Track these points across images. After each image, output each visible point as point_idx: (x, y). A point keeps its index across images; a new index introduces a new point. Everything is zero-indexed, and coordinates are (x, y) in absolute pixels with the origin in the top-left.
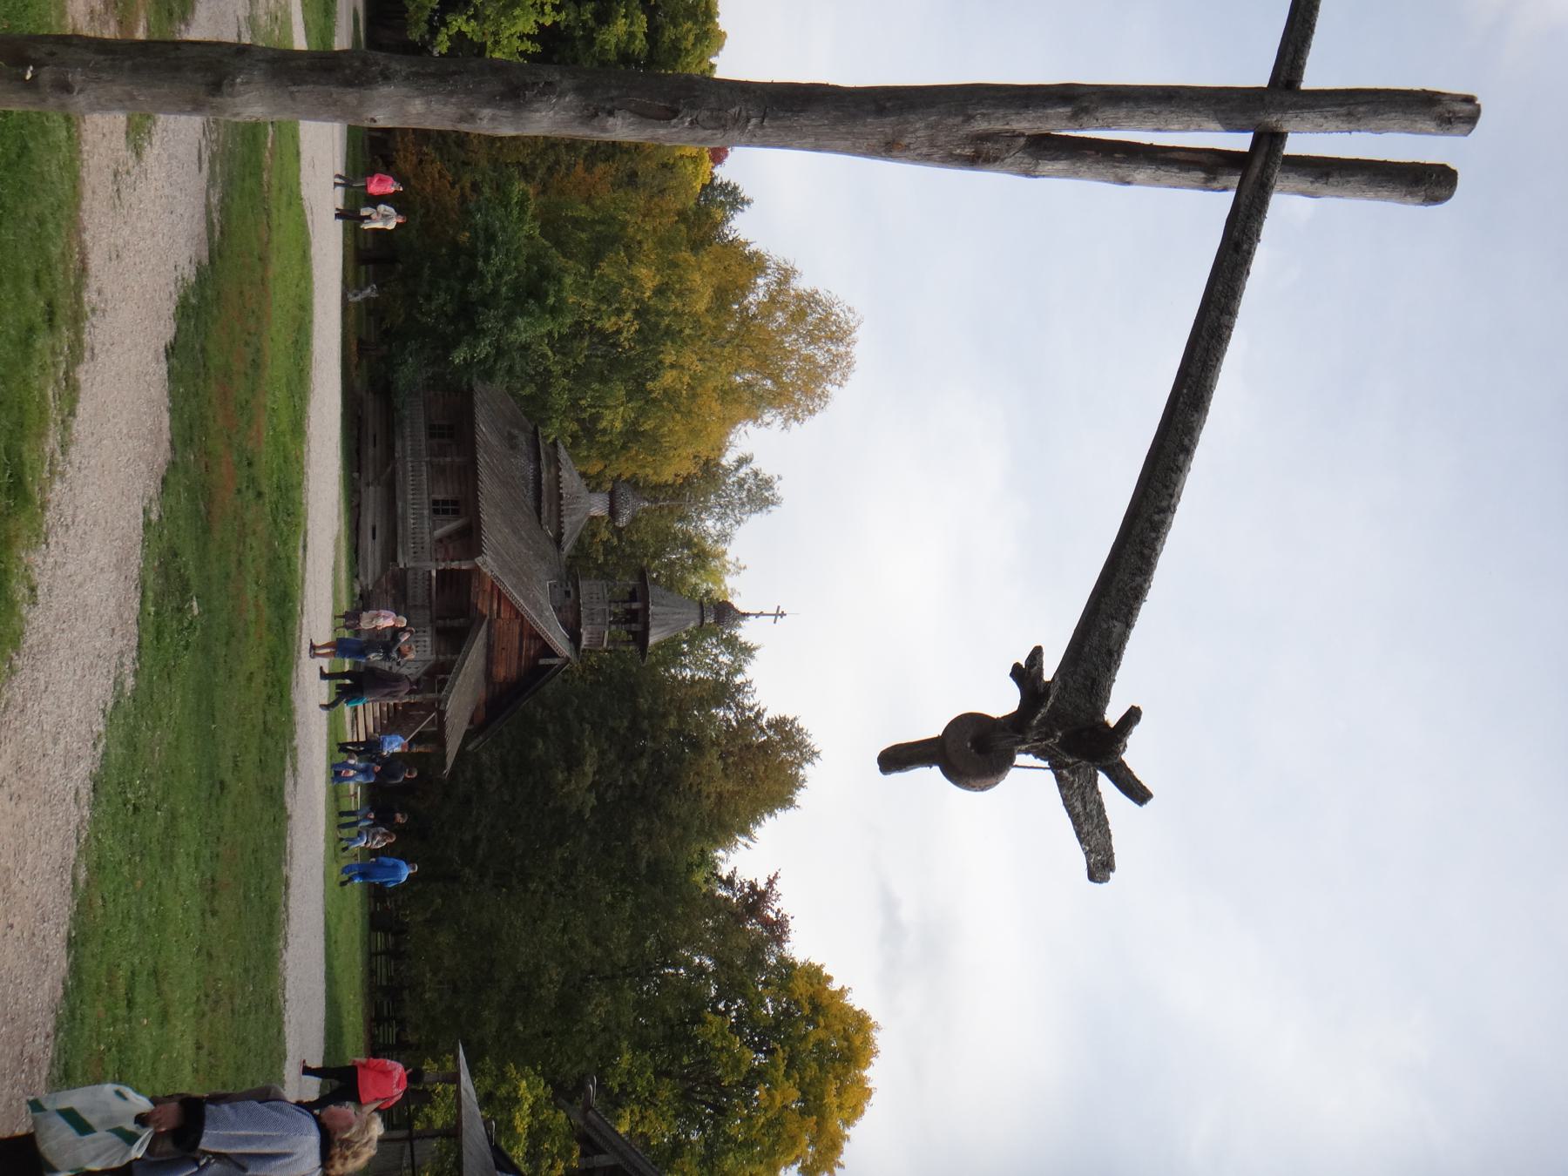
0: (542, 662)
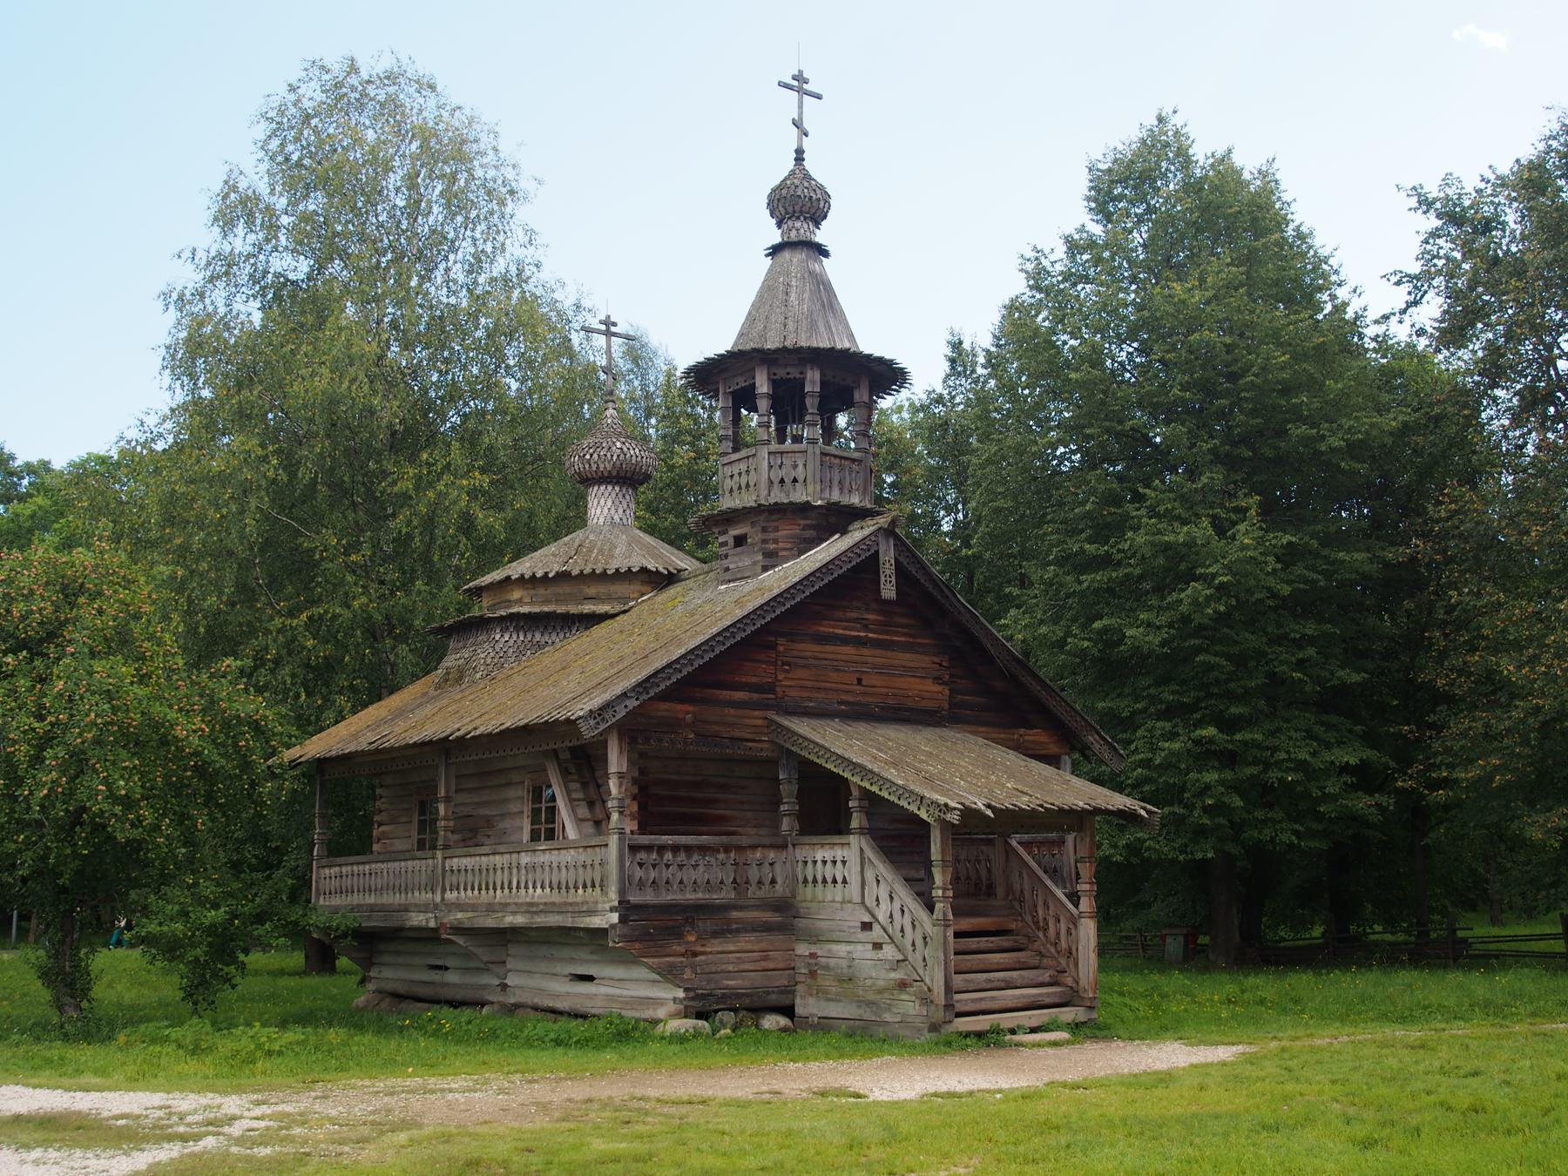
0: (888, 591)
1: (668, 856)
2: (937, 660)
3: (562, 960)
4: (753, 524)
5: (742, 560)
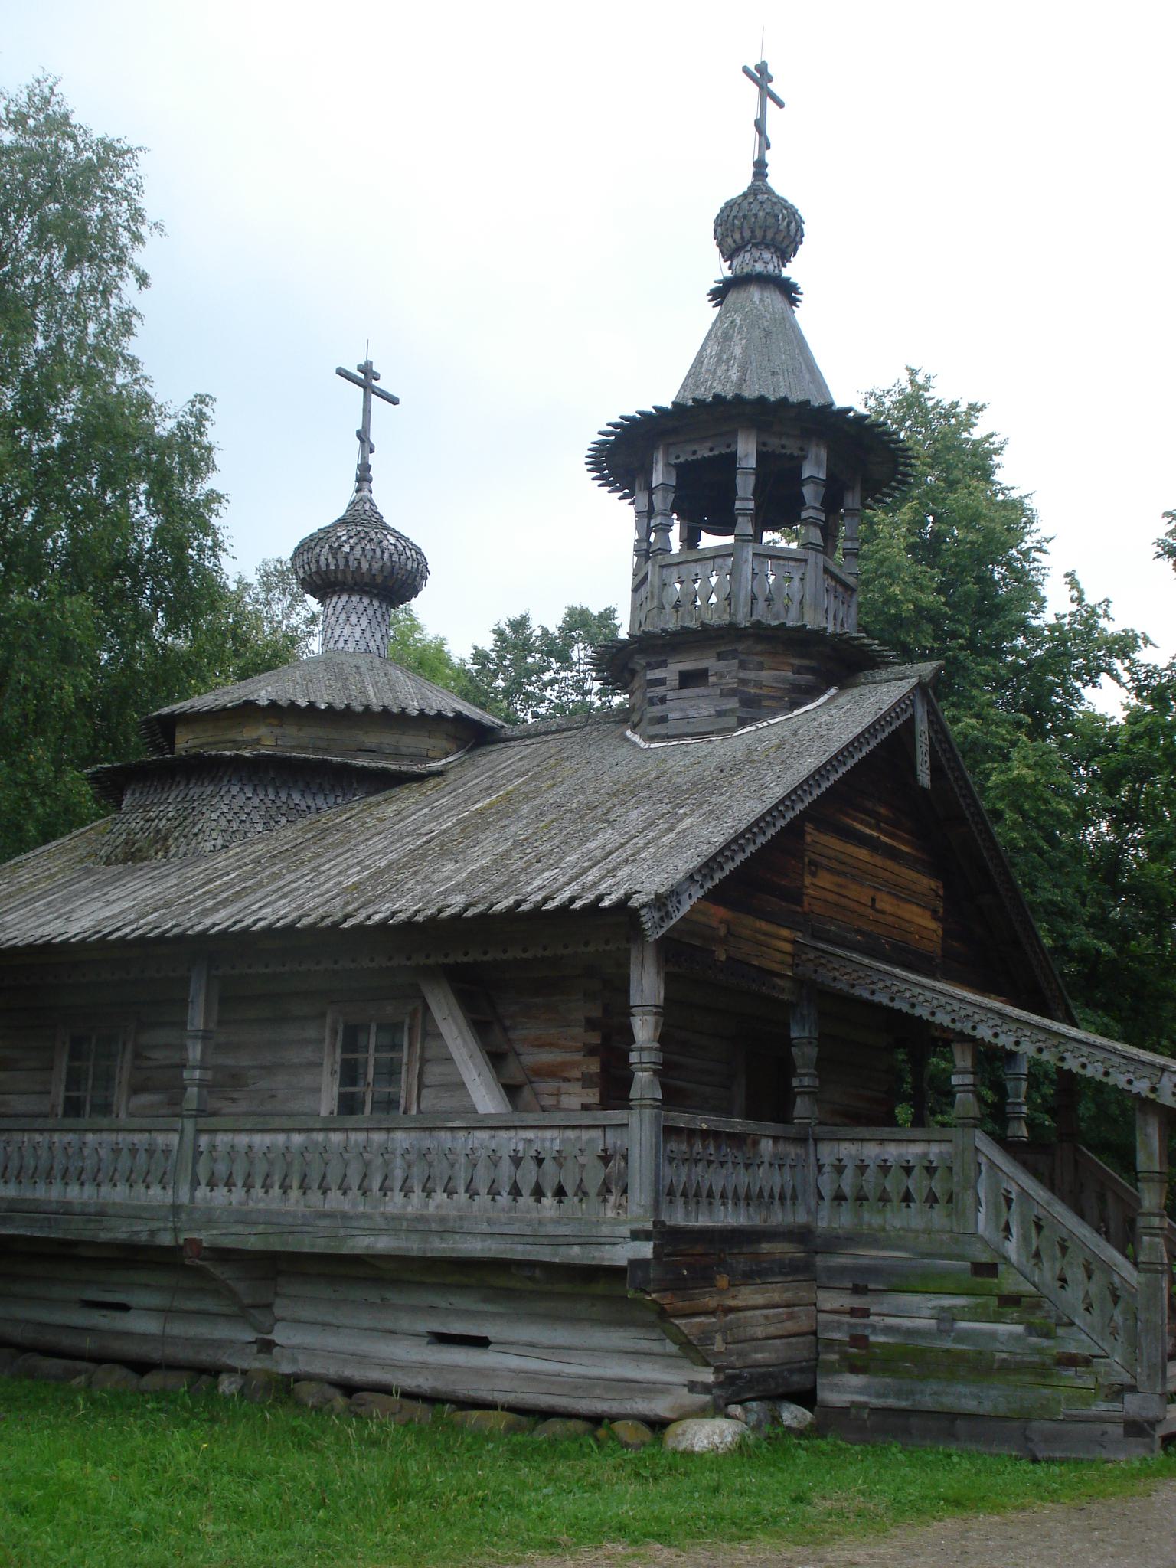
0: (925, 778)
1: (698, 1147)
2: (933, 884)
3: (413, 1310)
4: (720, 657)
5: (700, 705)
